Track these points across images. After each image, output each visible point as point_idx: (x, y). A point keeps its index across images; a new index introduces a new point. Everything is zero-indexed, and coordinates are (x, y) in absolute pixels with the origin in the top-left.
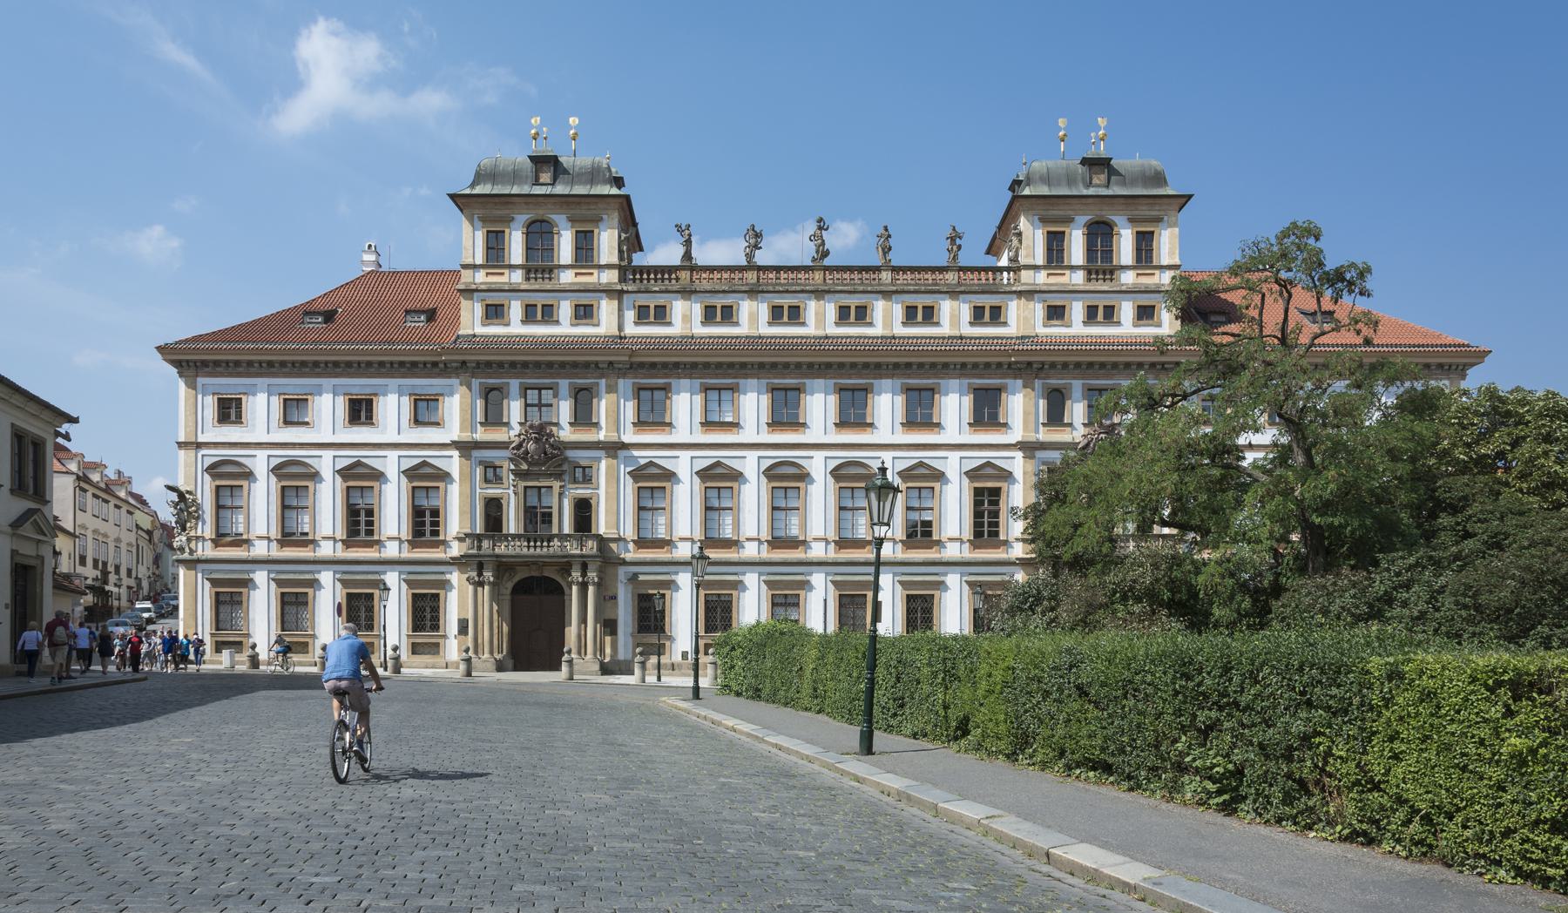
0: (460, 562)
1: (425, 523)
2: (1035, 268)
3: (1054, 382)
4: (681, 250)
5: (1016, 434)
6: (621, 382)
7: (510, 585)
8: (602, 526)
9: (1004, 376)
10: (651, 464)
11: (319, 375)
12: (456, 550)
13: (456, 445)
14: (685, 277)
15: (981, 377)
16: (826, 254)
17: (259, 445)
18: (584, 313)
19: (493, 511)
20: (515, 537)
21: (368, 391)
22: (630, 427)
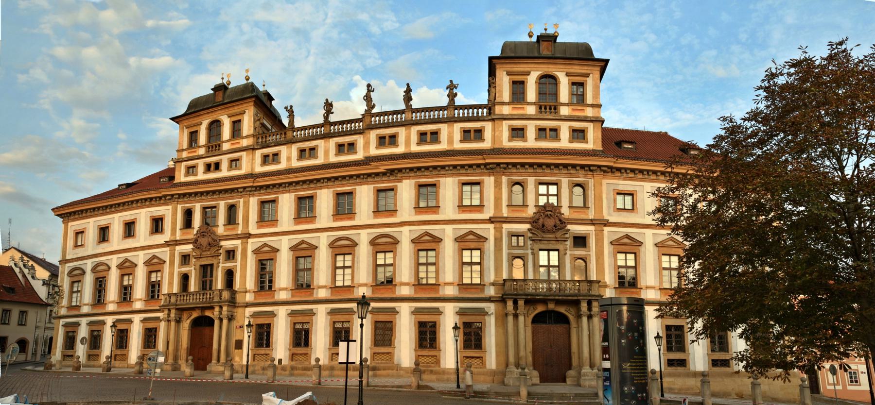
3: (516, 178)
8: (237, 286)
9: (482, 174)
15: (467, 175)
19: (185, 278)
20: (193, 294)
22: (255, 225)
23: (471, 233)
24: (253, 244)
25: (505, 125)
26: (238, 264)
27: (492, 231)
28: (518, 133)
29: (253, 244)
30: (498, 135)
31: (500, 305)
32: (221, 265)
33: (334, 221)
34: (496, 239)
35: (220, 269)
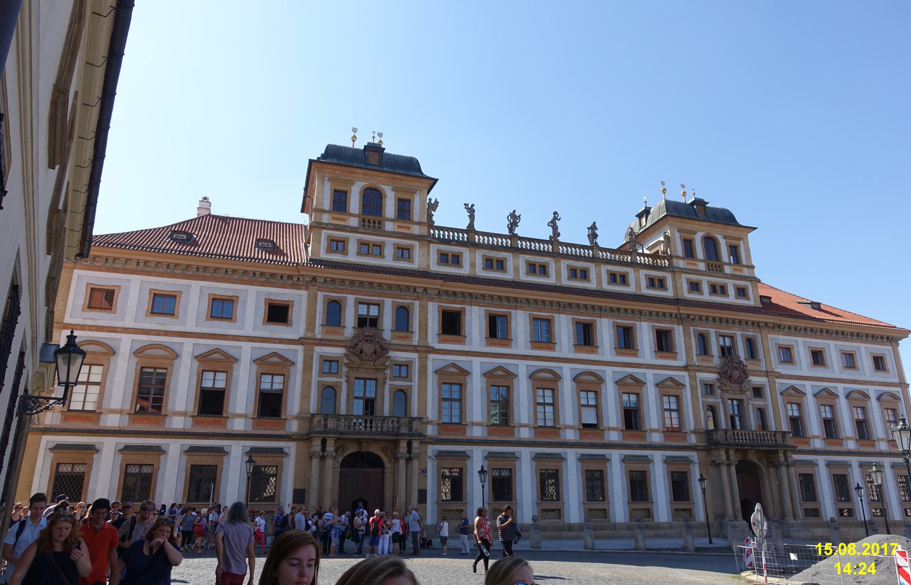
0: (304, 438)
1: (270, 404)
2: (679, 258)
4: (468, 221)
5: (681, 362)
6: (430, 304)
7: (340, 459)
10: (454, 365)
11: (189, 277)
12: (294, 427)
13: (299, 341)
14: (470, 237)
16: (559, 235)
17: (126, 330)
18: (404, 252)
21: (230, 294)
22: (436, 338)
23: (671, 379)
24: (434, 362)
25: (684, 276)
26: (415, 384)
27: (687, 379)
28: (695, 287)
29: (434, 362)
30: (676, 287)
31: (703, 454)
32: (388, 382)
33: (532, 348)
34: (692, 387)
35: (387, 387)
